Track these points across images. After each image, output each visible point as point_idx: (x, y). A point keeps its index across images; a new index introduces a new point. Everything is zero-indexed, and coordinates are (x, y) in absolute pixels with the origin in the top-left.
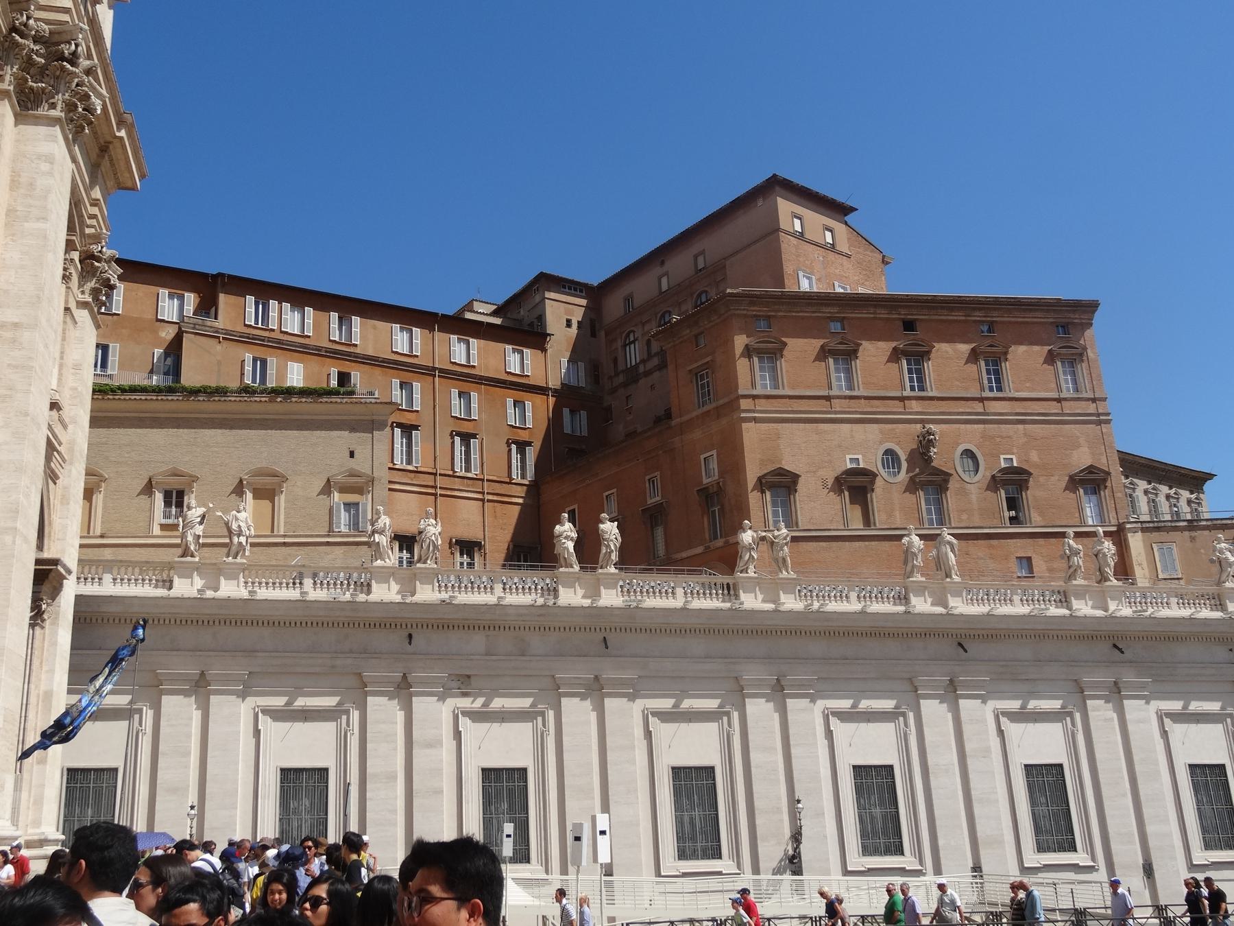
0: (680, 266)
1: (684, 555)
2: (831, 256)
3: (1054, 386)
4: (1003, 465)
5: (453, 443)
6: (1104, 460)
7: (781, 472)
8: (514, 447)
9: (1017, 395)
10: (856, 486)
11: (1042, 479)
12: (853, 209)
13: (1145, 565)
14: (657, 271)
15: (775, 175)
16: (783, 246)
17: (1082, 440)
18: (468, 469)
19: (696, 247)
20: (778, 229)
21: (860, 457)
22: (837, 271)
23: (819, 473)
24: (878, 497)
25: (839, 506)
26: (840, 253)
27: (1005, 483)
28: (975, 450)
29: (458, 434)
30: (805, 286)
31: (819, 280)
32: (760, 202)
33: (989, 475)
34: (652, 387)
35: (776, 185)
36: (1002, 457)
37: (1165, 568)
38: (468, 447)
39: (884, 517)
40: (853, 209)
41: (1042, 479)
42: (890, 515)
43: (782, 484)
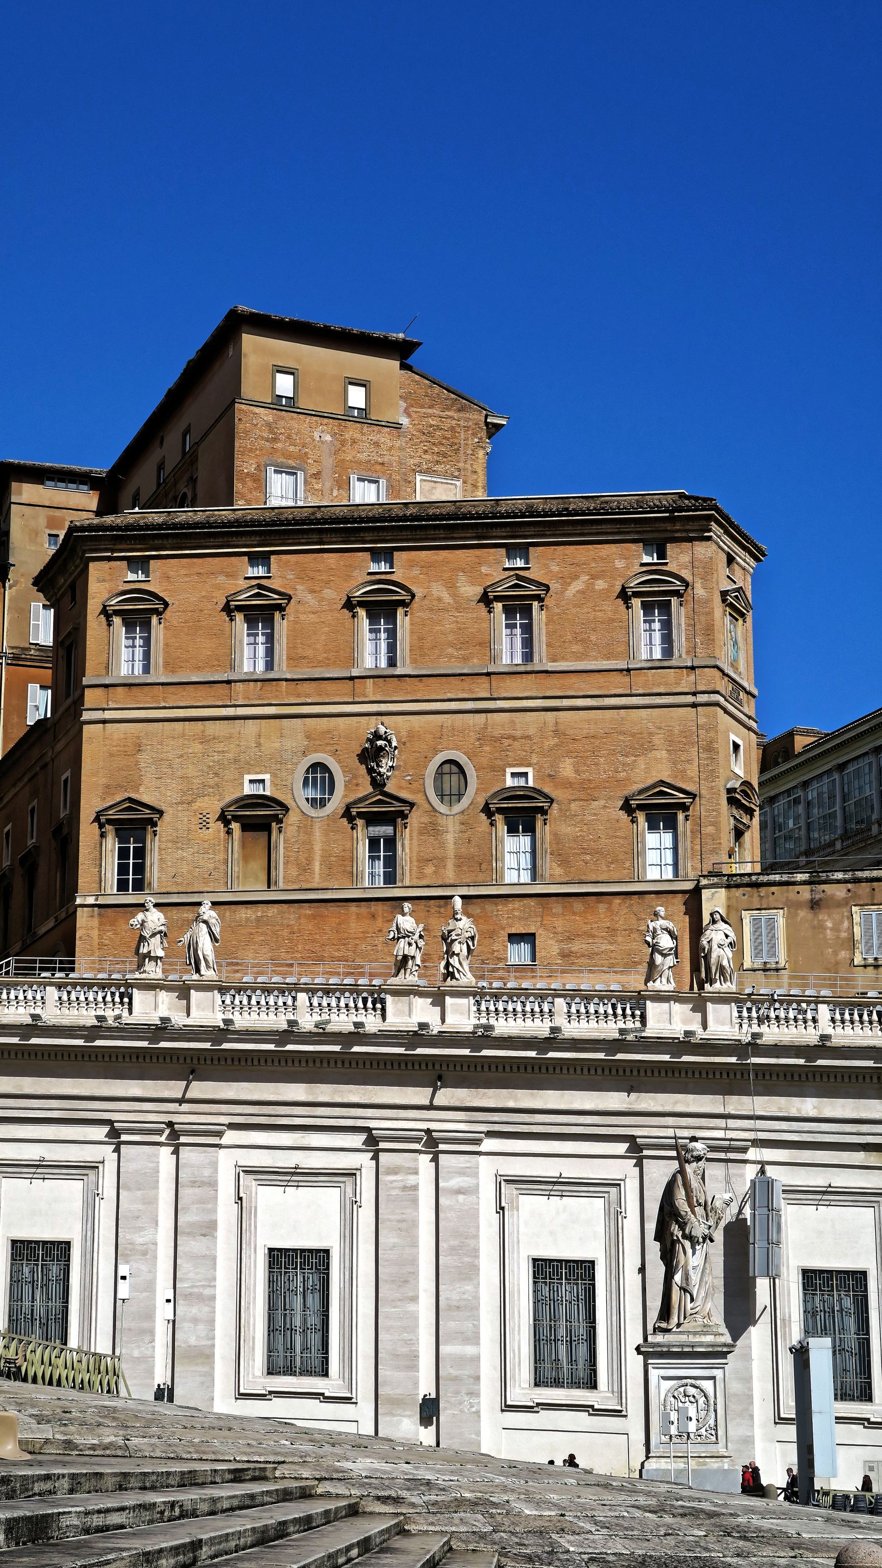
3: (621, 648)
4: (510, 782)
6: (692, 770)
9: (551, 666)
17: (657, 740)
23: (195, 806)
28: (463, 759)
36: (509, 770)
37: (757, 951)
39: (294, 872)
42: (305, 869)
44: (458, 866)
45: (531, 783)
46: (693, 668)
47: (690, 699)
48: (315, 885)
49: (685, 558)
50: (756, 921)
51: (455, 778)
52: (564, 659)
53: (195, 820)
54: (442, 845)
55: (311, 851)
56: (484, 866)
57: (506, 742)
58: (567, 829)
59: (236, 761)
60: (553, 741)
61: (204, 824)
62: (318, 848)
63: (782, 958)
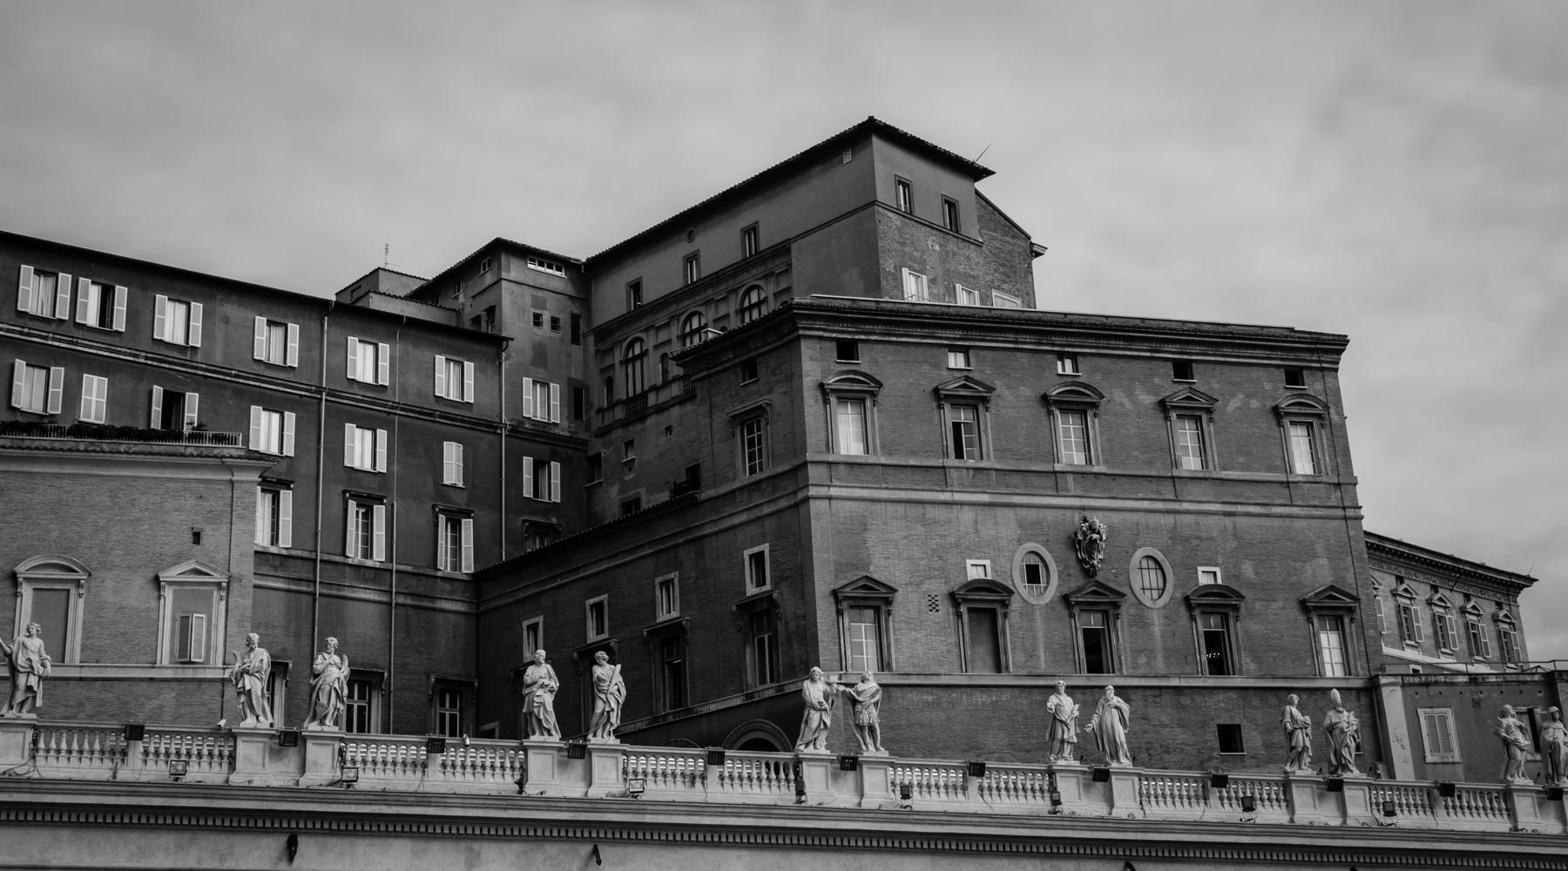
0: (719, 246)
1: (713, 708)
2: (952, 245)
3: (1278, 463)
4: (1204, 580)
5: (346, 510)
6: (1350, 578)
7: (870, 584)
8: (442, 518)
10: (982, 607)
11: (1258, 605)
12: (986, 173)
13: (1406, 742)
14: (682, 249)
15: (871, 119)
16: (881, 228)
17: (1319, 547)
18: (368, 553)
19: (745, 218)
20: (874, 203)
21: (987, 563)
22: (961, 268)
23: (924, 587)
24: (1012, 627)
25: (953, 639)
26: (967, 240)
27: (1207, 610)
28: (1160, 556)
29: (354, 496)
30: (914, 289)
31: (932, 281)
32: (847, 158)
33: (1179, 595)
34: (669, 429)
35: (871, 129)
36: (1200, 569)
37: (1435, 749)
38: (368, 516)
39: (1021, 658)
40: (986, 173)
41: (1258, 605)
42: (1031, 655)
43: (871, 599)
44: (1166, 658)
45: (1220, 581)
46: (1339, 485)
47: (1340, 512)
48: (1041, 671)
49: (1319, 386)
50: (1430, 718)
51: (1153, 572)
52: (1233, 468)
53: (925, 602)
54: (1151, 637)
55: (1034, 637)
56: (1190, 659)
57: (1195, 542)
58: (1254, 627)
59: (957, 546)
60: (1232, 544)
61: (934, 607)
62: (1040, 634)
63: (1457, 758)
